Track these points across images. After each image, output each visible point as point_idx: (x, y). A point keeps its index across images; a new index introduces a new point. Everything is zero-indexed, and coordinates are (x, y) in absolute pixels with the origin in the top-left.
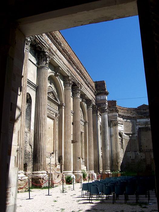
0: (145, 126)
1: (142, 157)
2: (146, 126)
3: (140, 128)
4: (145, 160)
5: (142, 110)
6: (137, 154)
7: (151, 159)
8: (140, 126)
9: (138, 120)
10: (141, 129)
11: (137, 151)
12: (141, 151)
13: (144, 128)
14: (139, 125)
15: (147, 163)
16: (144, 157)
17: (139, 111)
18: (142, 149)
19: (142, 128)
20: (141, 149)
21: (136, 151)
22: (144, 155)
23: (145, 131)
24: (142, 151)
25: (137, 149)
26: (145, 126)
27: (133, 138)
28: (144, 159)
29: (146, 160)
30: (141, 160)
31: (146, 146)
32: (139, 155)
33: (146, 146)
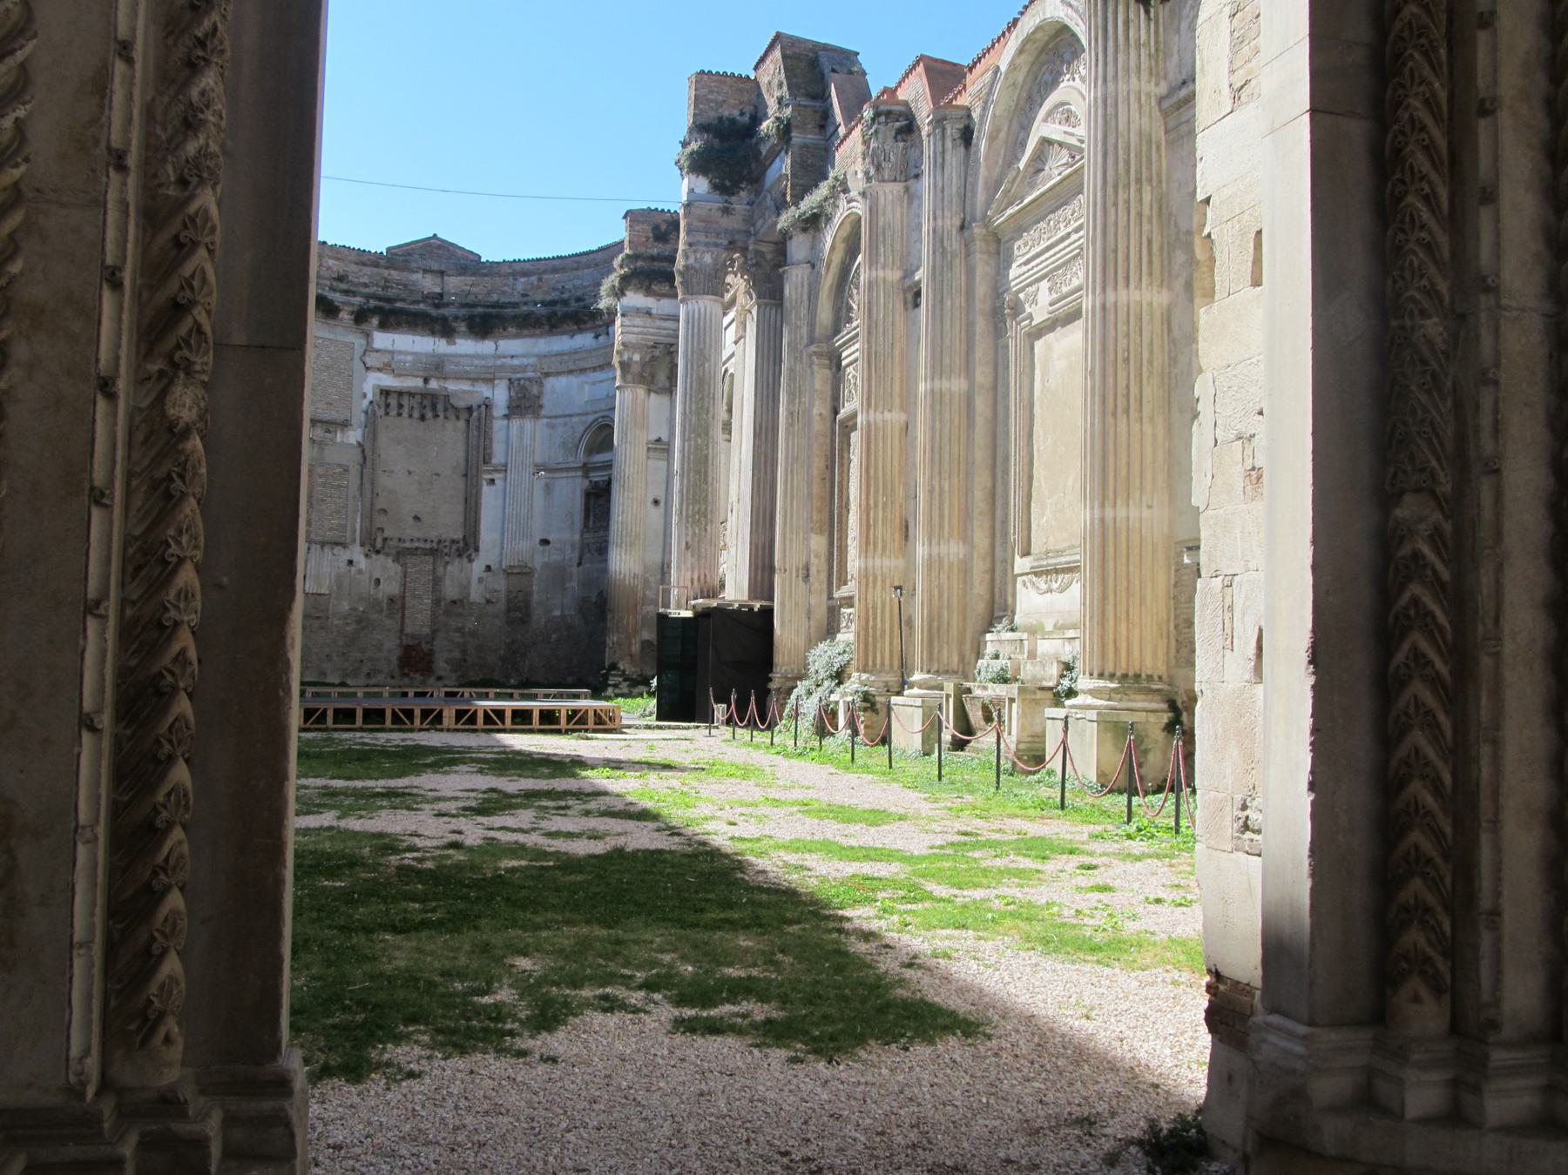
0: (426, 381)
1: (378, 581)
2: (434, 384)
3: (385, 393)
4: (397, 605)
5: (419, 276)
6: (350, 562)
7: (437, 602)
8: (388, 381)
9: (382, 340)
10: (393, 401)
11: (354, 541)
12: (373, 546)
13: (411, 394)
14: (379, 370)
15: (408, 630)
16: (391, 588)
17: (395, 274)
18: (387, 533)
19: (400, 394)
20: (382, 530)
21: (344, 545)
22: (394, 568)
23: (416, 414)
24: (379, 544)
25: (354, 532)
26: (426, 381)
27: (331, 455)
28: (391, 600)
29: (403, 608)
30: (375, 604)
31: (416, 518)
32: (360, 572)
33: (416, 518)
